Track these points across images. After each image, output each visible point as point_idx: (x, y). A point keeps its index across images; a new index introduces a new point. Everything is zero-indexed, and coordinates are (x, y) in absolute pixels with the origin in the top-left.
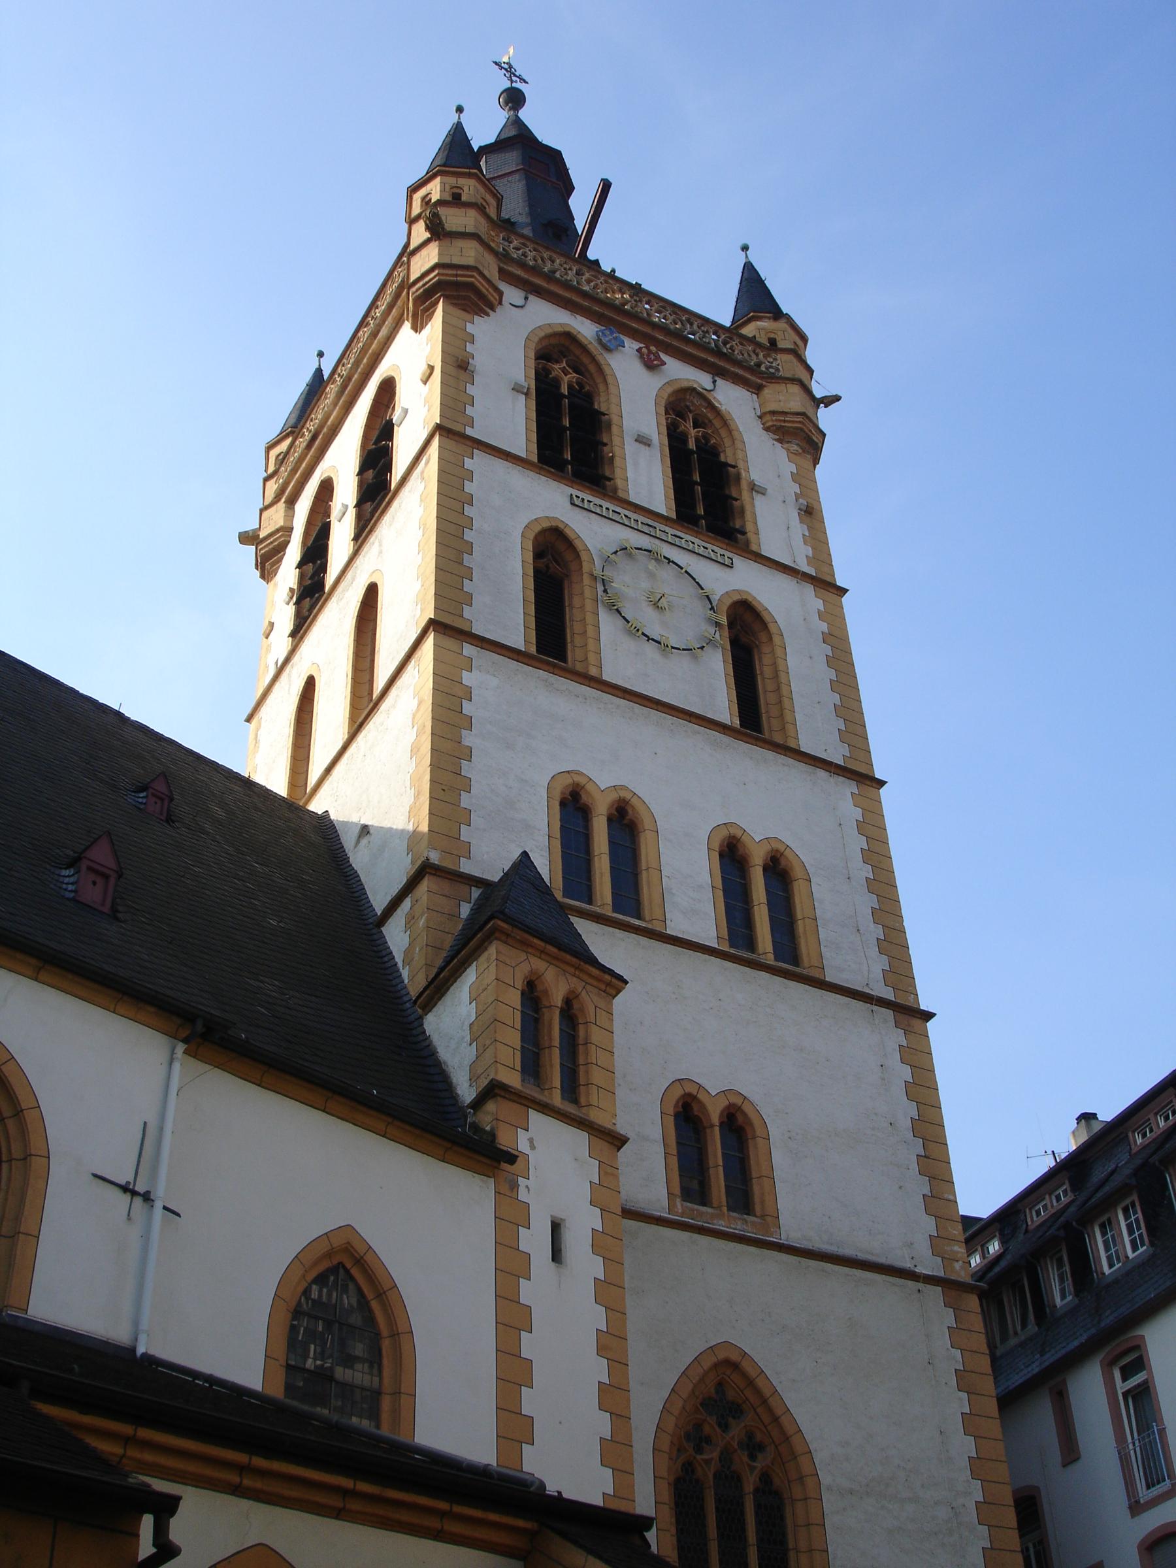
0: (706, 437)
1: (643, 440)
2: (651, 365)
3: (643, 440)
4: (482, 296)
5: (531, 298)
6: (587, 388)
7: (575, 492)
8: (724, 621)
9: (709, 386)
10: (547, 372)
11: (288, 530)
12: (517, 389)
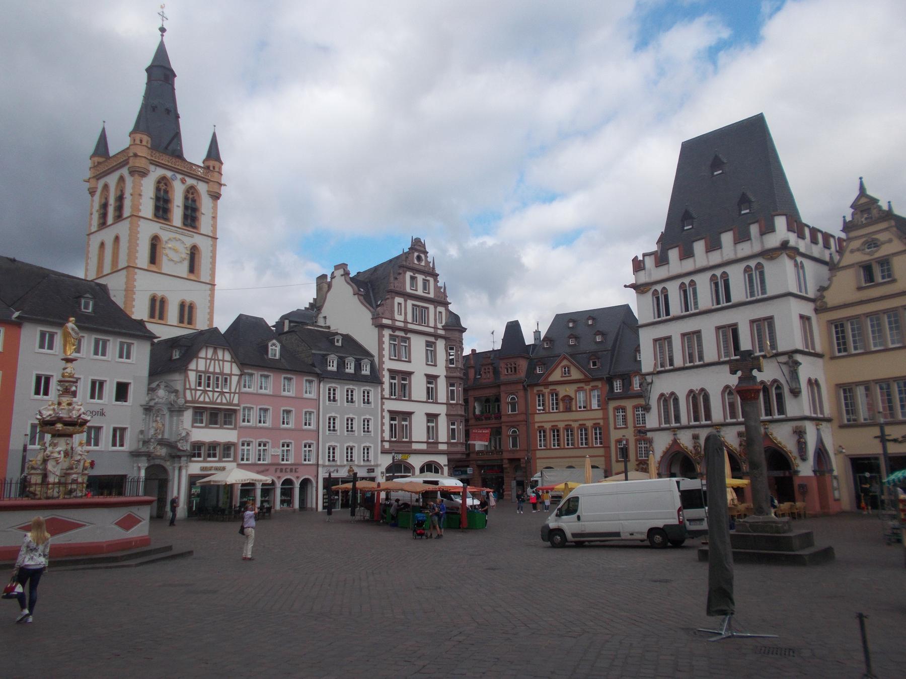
0: (194, 197)
1: (178, 206)
2: (183, 181)
3: (178, 206)
4: (145, 173)
6: (168, 189)
8: (189, 252)
9: (196, 184)
10: (159, 186)
11: (97, 188)
12: (151, 198)
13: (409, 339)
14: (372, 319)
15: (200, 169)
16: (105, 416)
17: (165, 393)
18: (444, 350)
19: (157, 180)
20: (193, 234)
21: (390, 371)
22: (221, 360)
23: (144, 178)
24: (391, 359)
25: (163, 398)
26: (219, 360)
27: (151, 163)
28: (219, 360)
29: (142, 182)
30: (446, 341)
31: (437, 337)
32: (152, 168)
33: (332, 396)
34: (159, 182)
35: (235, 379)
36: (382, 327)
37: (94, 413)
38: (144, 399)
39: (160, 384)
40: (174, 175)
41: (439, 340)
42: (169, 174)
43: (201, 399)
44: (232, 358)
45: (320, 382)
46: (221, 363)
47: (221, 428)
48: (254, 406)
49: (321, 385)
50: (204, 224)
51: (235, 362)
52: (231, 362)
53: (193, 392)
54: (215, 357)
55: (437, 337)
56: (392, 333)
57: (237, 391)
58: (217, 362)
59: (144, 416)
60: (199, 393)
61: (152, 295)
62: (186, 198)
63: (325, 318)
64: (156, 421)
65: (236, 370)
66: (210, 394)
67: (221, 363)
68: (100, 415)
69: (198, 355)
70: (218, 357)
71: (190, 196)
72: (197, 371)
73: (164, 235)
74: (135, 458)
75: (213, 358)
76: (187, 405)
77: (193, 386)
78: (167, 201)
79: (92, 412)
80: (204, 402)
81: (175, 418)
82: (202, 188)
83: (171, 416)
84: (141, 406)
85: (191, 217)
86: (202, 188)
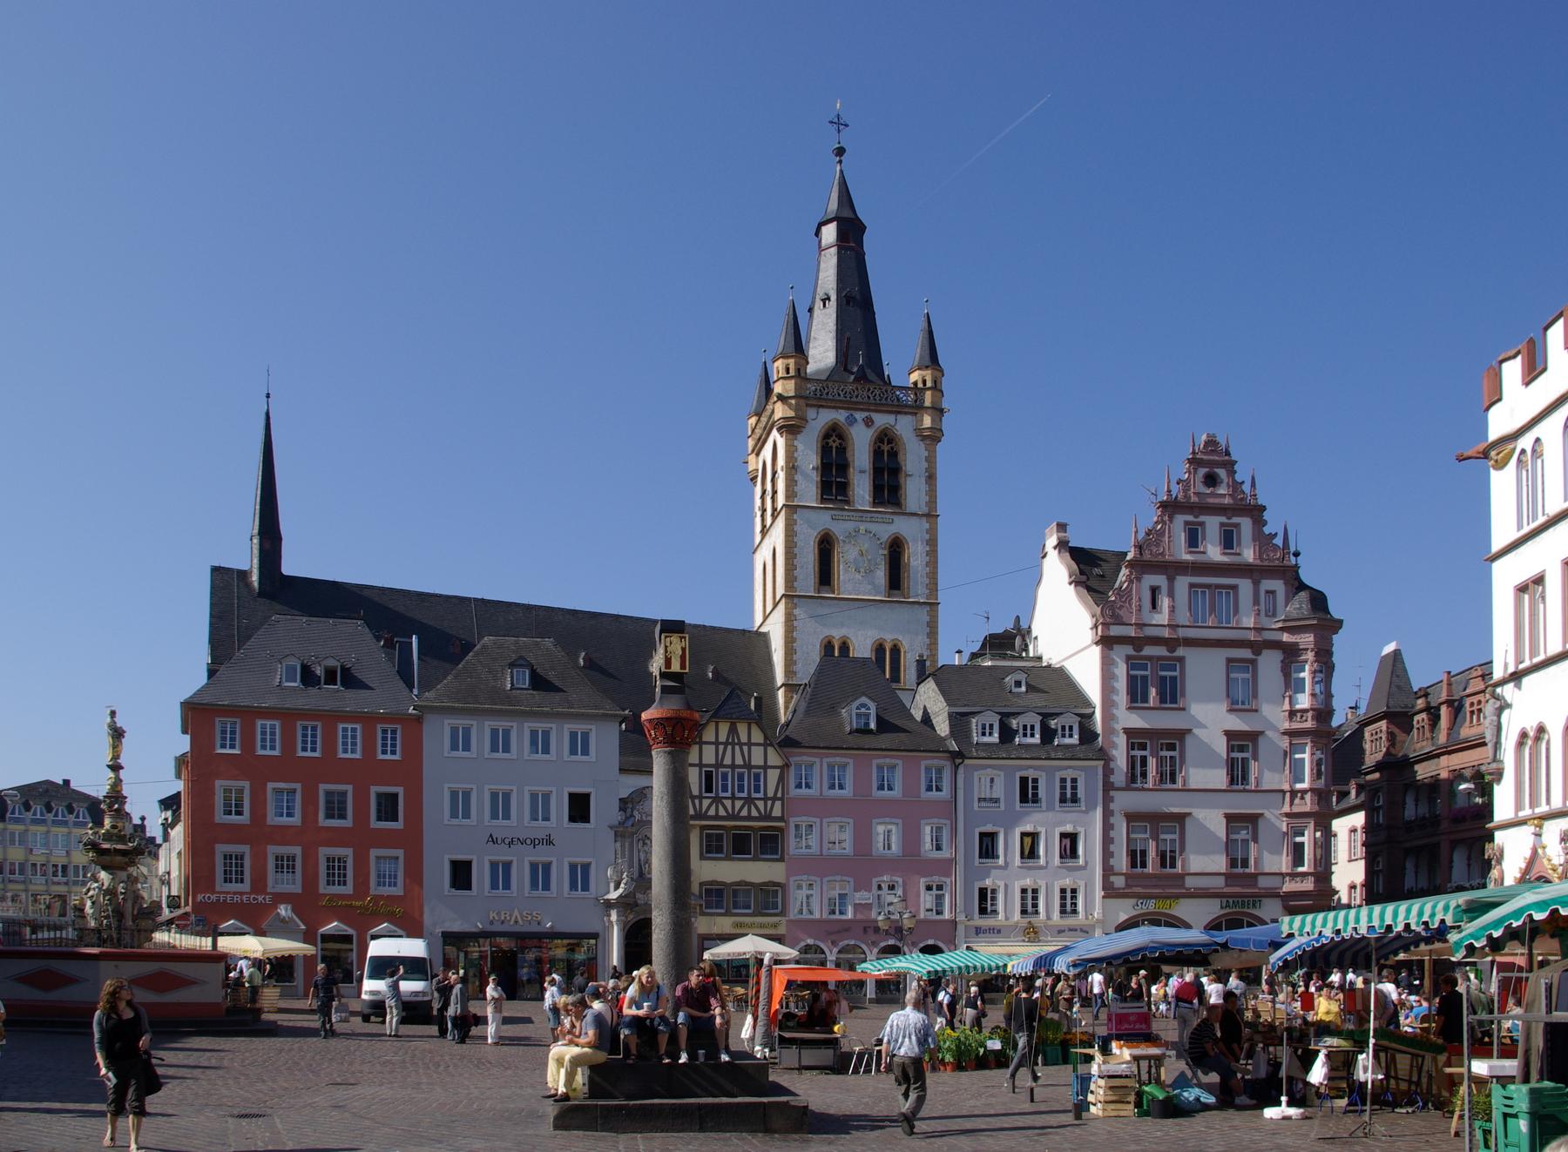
0: (892, 448)
2: (869, 422)
3: (864, 472)
4: (799, 427)
5: (821, 410)
7: (833, 512)
8: (886, 552)
10: (827, 443)
13: (1181, 660)
14: (1092, 629)
15: (898, 393)
18: (1281, 674)
19: (823, 430)
20: (892, 517)
21: (1129, 732)
22: (745, 744)
23: (798, 436)
24: (1129, 708)
26: (741, 744)
27: (807, 405)
28: (741, 744)
29: (796, 443)
30: (1284, 653)
31: (1258, 647)
32: (811, 413)
33: (1069, 791)
34: (827, 436)
35: (773, 776)
36: (1106, 642)
38: (616, 816)
40: (852, 415)
41: (1266, 653)
42: (840, 416)
43: (712, 812)
44: (766, 738)
45: (957, 767)
46: (745, 748)
47: (755, 859)
48: (818, 820)
49: (961, 770)
50: (913, 492)
51: (771, 745)
52: (765, 745)
53: (697, 802)
54: (733, 740)
55: (1258, 647)
56: (1134, 653)
57: (779, 795)
58: (737, 748)
60: (706, 803)
61: (827, 640)
62: (877, 454)
63: (1036, 638)
65: (774, 758)
66: (728, 803)
67: (745, 748)
69: (701, 738)
70: (739, 739)
71: (886, 448)
72: (700, 765)
73: (839, 529)
75: (730, 741)
77: (695, 792)
78: (843, 467)
79: (533, 841)
80: (717, 817)
82: (903, 426)
85: (888, 488)
86: (903, 426)
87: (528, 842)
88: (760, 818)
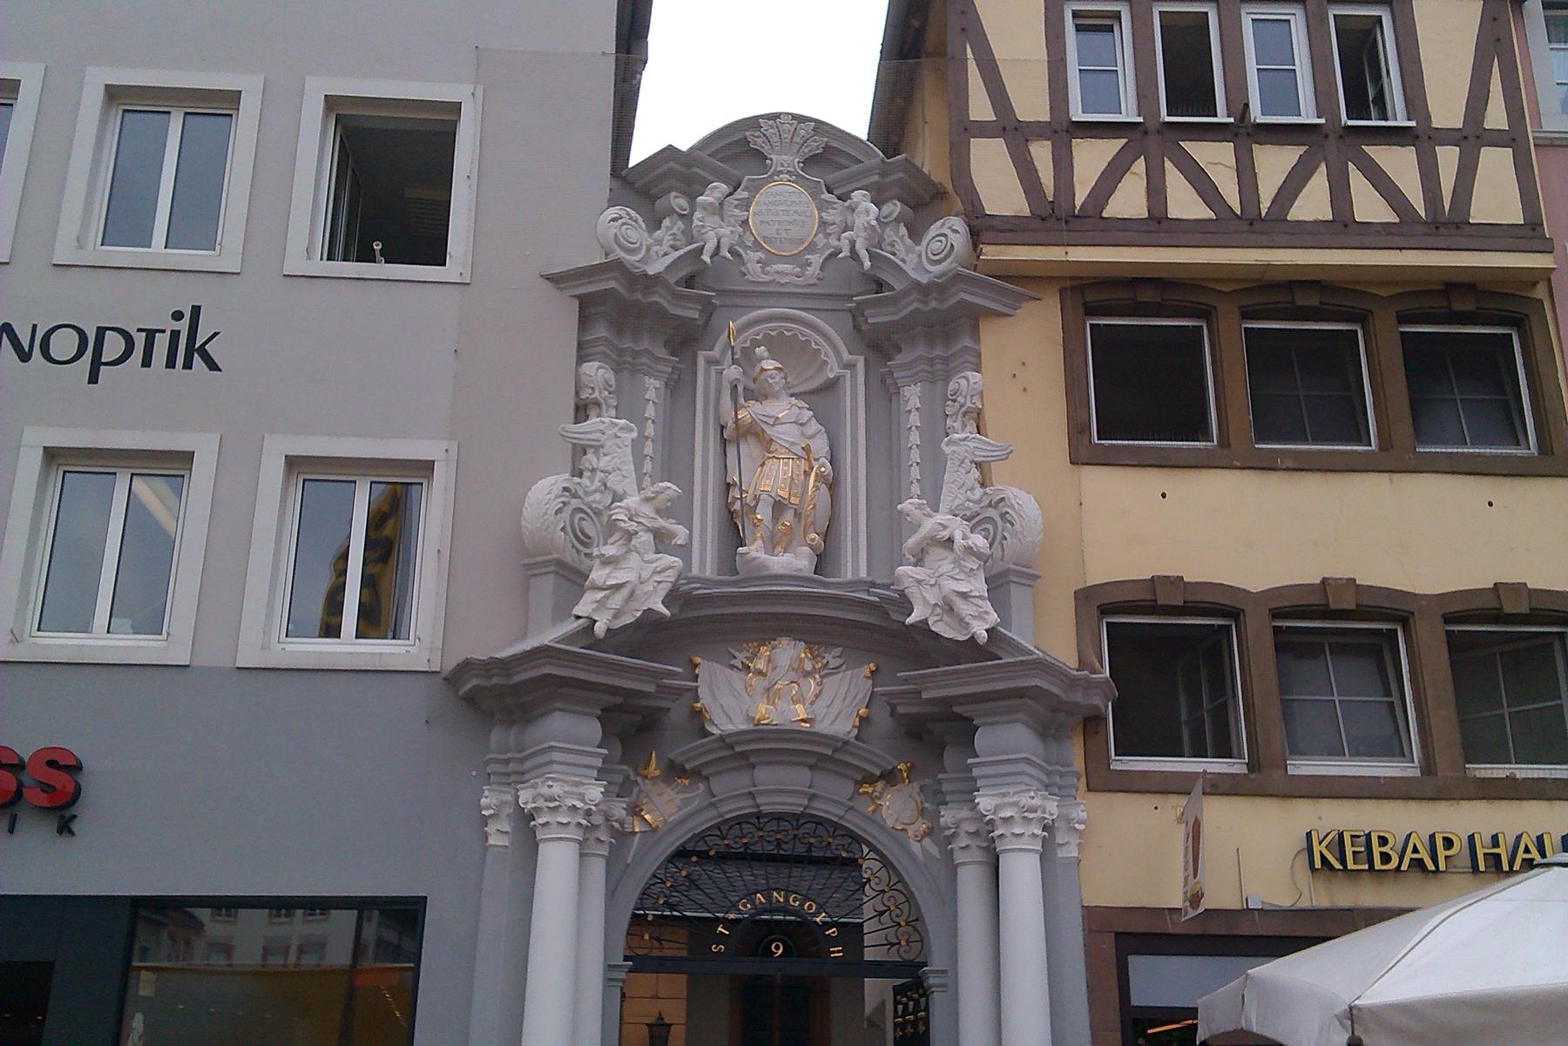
16: (213, 366)
17: (822, 206)
25: (811, 248)
37: (113, 346)
39: (758, 142)
43: (1129, 201)
59: (595, 371)
60: (1091, 158)
64: (754, 432)
68: (171, 363)
74: (496, 736)
76: (991, 253)
79: (91, 347)
81: (913, 395)
83: (884, 392)
84: (550, 278)
87: (64, 344)
88: (1405, 230)
